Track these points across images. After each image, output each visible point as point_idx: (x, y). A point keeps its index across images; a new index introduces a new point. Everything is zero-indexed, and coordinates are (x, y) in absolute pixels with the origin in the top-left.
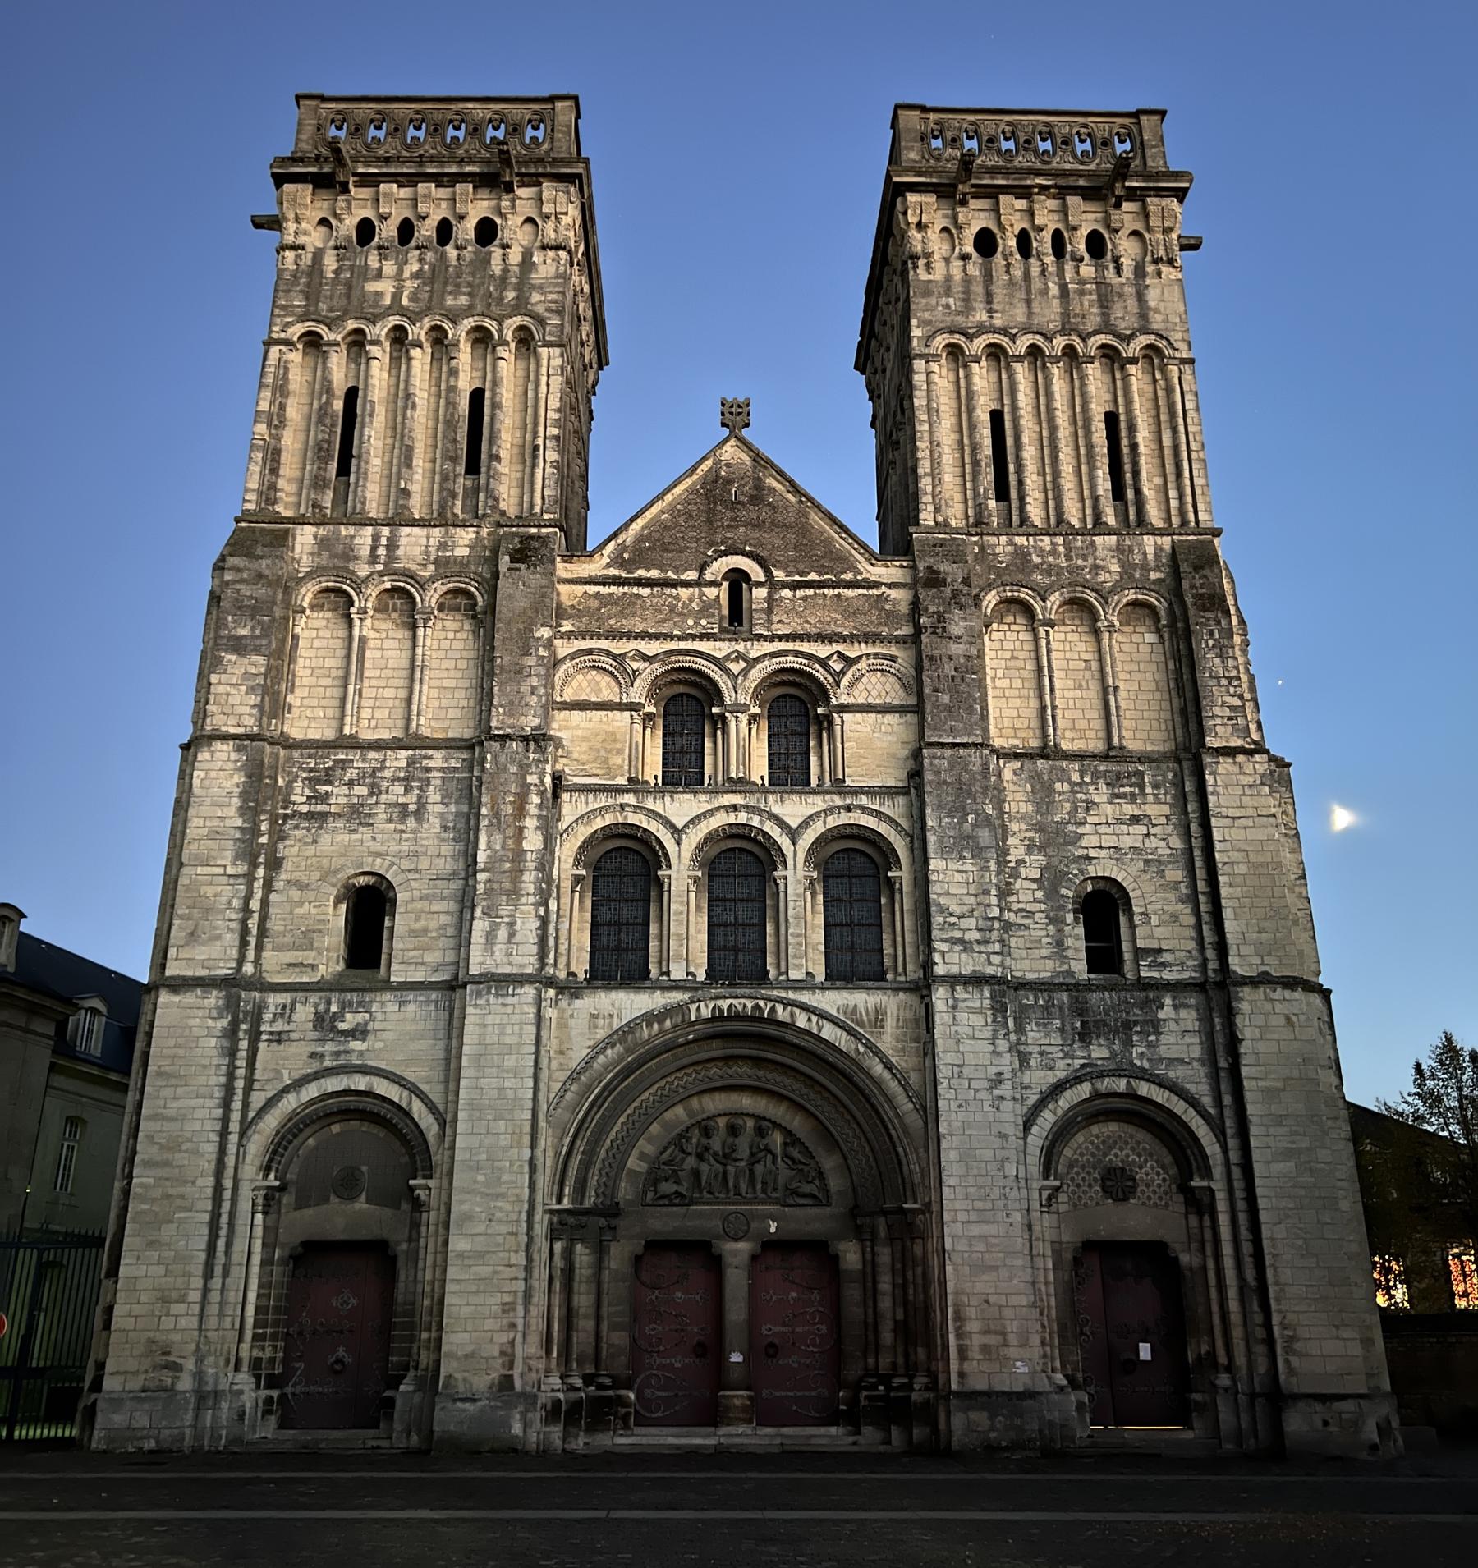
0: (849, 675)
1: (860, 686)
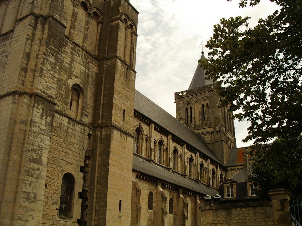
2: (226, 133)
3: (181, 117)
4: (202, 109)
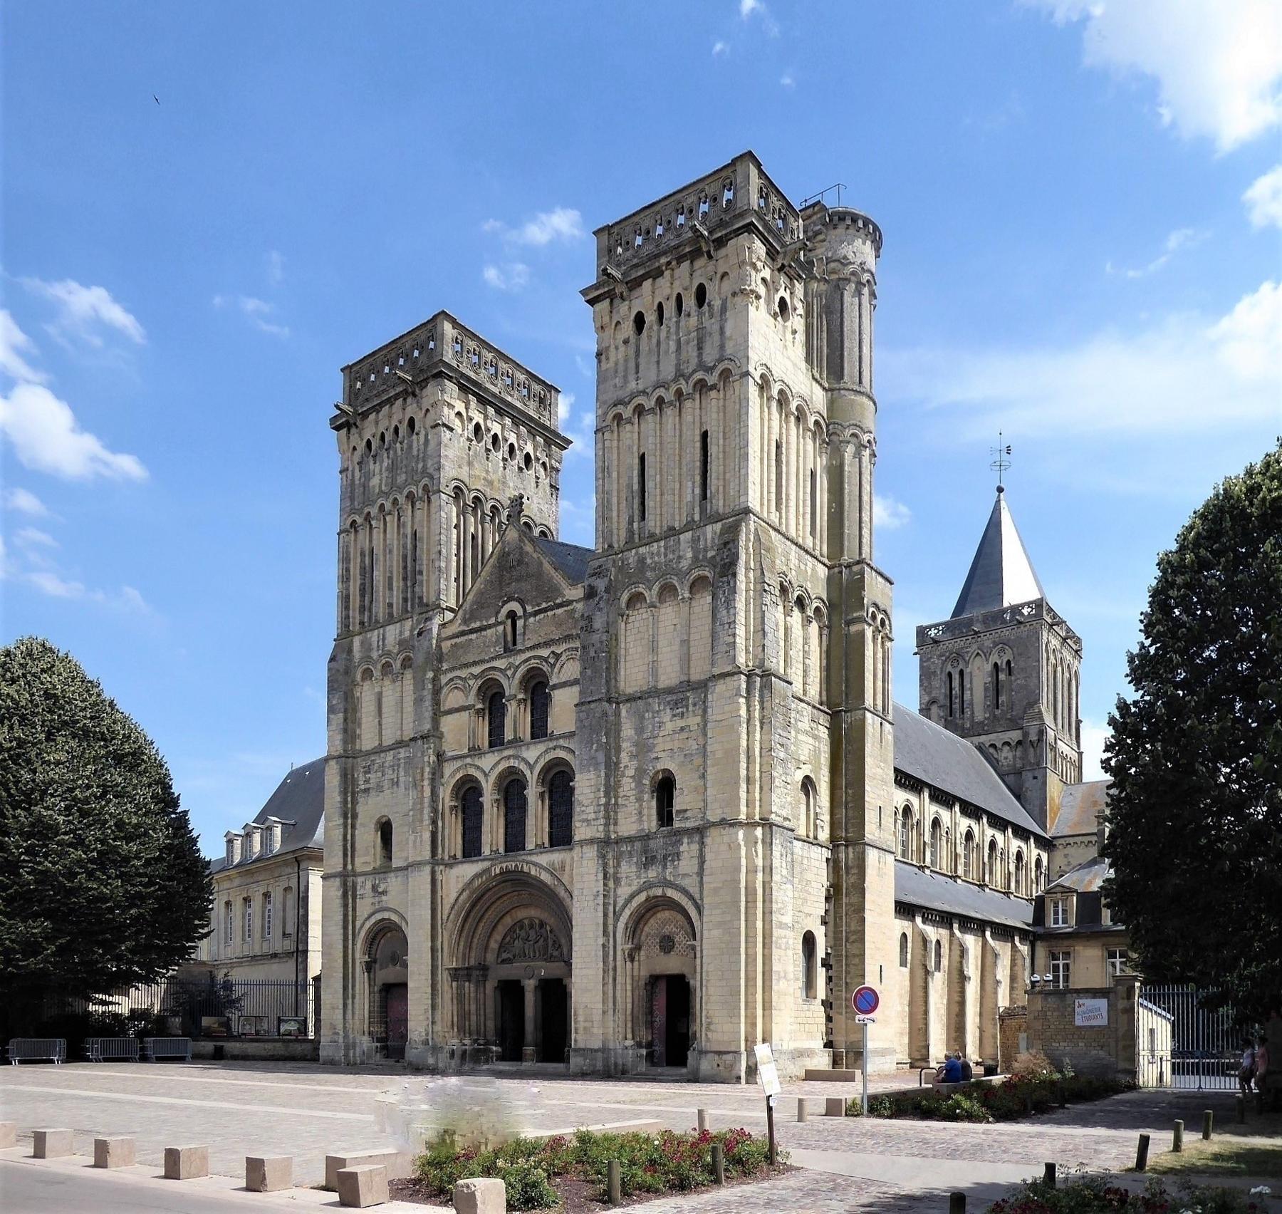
0: (558, 666)
1: (563, 670)
2: (1056, 743)
3: (934, 698)
4: (992, 677)
